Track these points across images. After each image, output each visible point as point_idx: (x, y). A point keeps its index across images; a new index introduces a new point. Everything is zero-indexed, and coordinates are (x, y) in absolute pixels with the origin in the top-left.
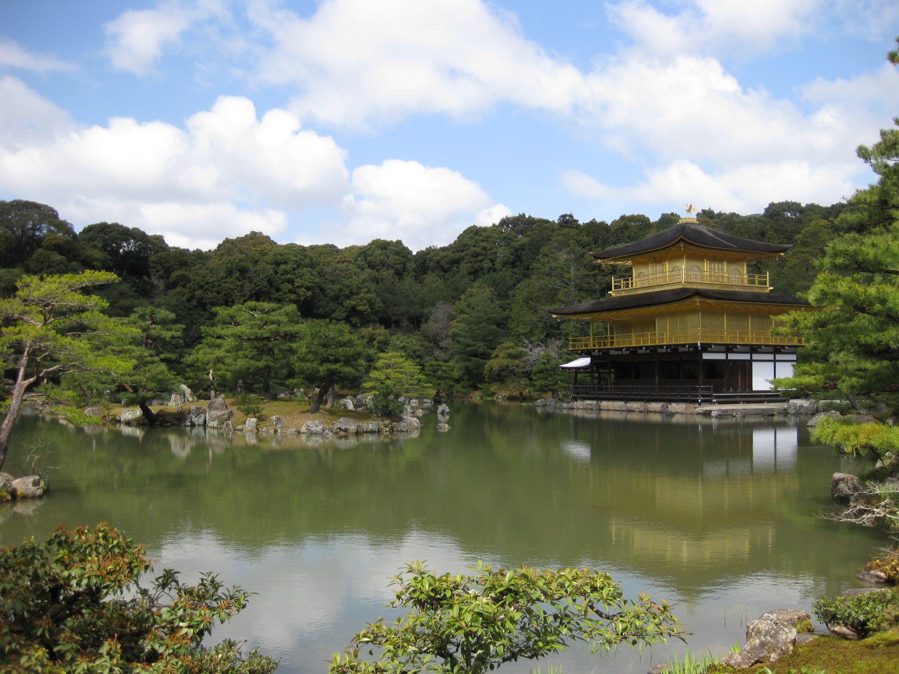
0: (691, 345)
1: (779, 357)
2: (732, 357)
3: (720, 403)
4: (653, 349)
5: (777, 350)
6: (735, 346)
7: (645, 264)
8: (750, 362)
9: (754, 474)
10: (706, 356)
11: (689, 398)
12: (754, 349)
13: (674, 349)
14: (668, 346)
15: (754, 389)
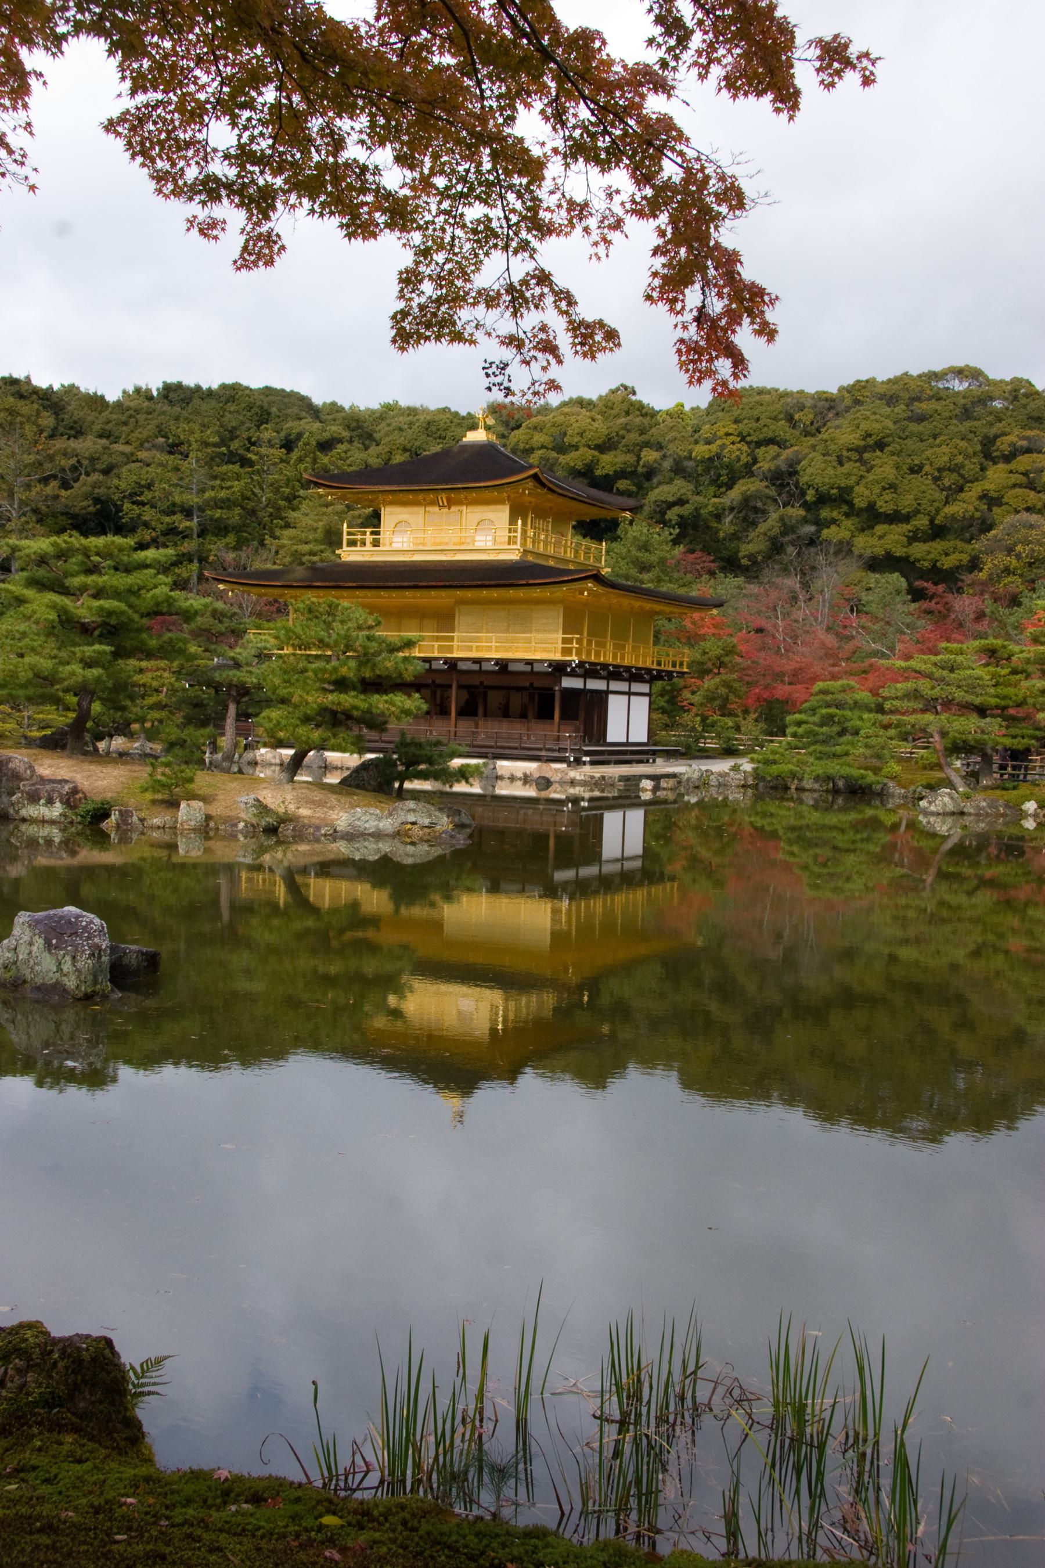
0: (551, 663)
1: (637, 687)
2: (595, 685)
3: (593, 763)
4: (452, 664)
5: (635, 675)
6: (605, 666)
7: (392, 503)
8: (607, 692)
9: (606, 884)
10: (568, 683)
11: (543, 753)
12: (615, 673)
13: (503, 665)
14: (498, 662)
15: (609, 739)
